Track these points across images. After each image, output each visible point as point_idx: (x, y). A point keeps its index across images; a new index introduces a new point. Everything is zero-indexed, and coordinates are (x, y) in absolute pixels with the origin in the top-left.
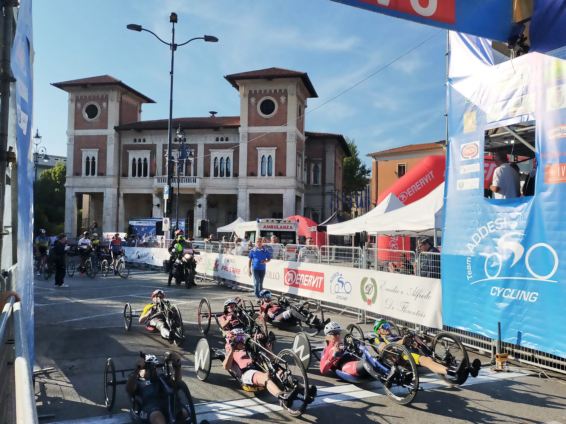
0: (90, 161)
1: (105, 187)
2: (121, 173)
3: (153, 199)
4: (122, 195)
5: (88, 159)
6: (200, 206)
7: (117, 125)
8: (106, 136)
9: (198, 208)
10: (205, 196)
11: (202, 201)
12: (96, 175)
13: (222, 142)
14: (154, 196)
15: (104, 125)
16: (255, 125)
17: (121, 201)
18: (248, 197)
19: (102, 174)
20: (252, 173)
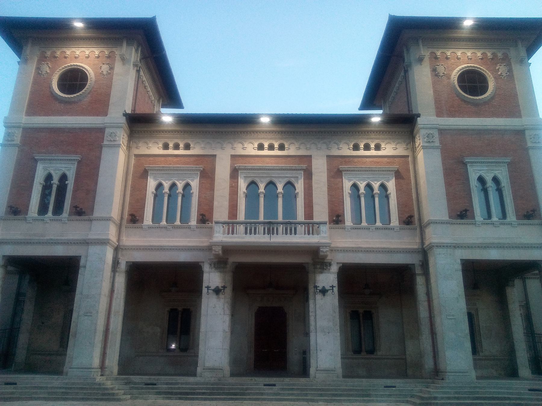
0: (55, 181)
1: (86, 243)
2: (126, 216)
3: (206, 276)
4: (123, 266)
5: (49, 177)
6: (324, 291)
7: (129, 111)
8: (100, 131)
9: (319, 297)
10: (335, 268)
11: (328, 279)
12: (65, 214)
13: (367, 153)
14: (206, 268)
15: (100, 105)
16: (452, 114)
17: (121, 281)
18: (459, 267)
19: (79, 212)
20: (462, 214)
